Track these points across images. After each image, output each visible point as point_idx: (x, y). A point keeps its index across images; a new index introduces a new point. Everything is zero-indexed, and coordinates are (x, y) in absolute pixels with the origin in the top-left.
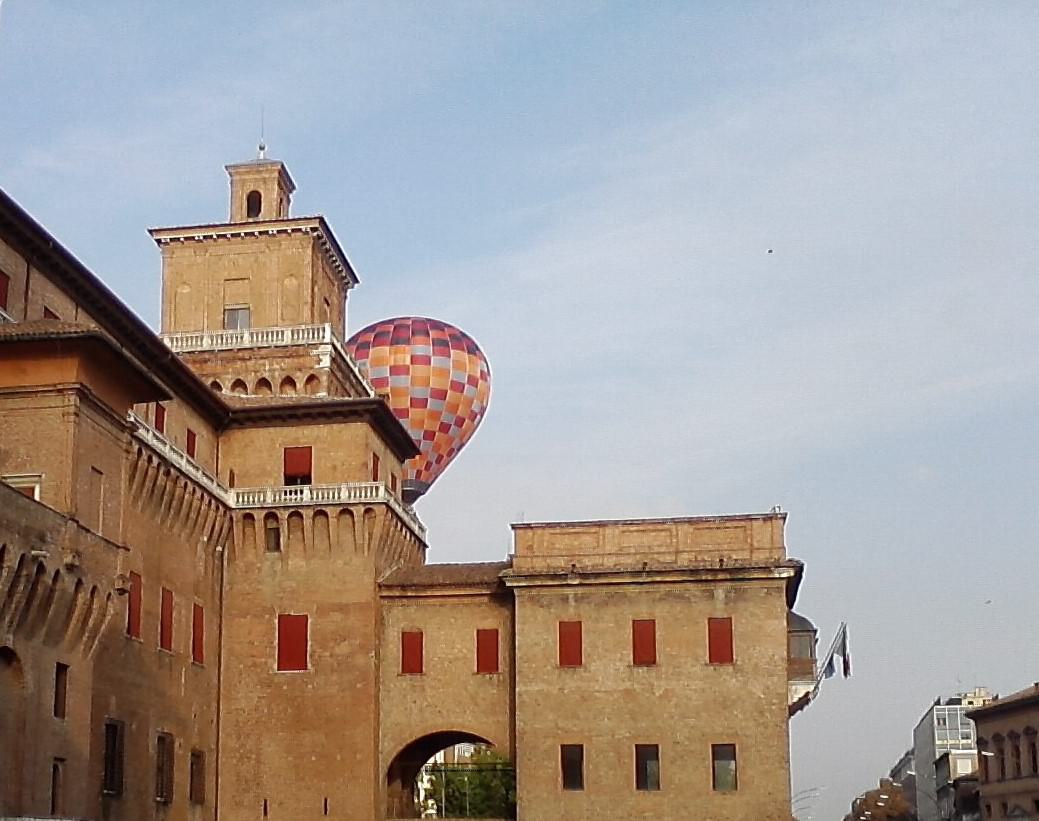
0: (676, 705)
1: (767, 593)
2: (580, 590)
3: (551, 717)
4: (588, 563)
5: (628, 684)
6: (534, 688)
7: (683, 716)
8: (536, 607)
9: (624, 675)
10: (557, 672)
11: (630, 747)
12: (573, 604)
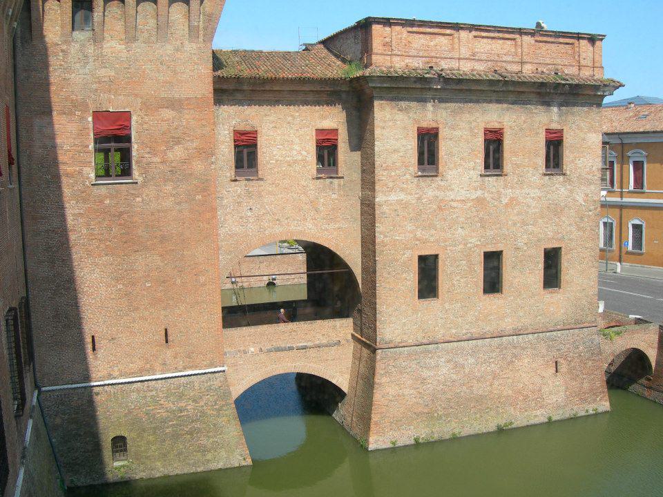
0: (519, 214)
3: (410, 227)
5: (479, 193)
6: (393, 197)
7: (524, 223)
9: (477, 184)
12: (431, 109)
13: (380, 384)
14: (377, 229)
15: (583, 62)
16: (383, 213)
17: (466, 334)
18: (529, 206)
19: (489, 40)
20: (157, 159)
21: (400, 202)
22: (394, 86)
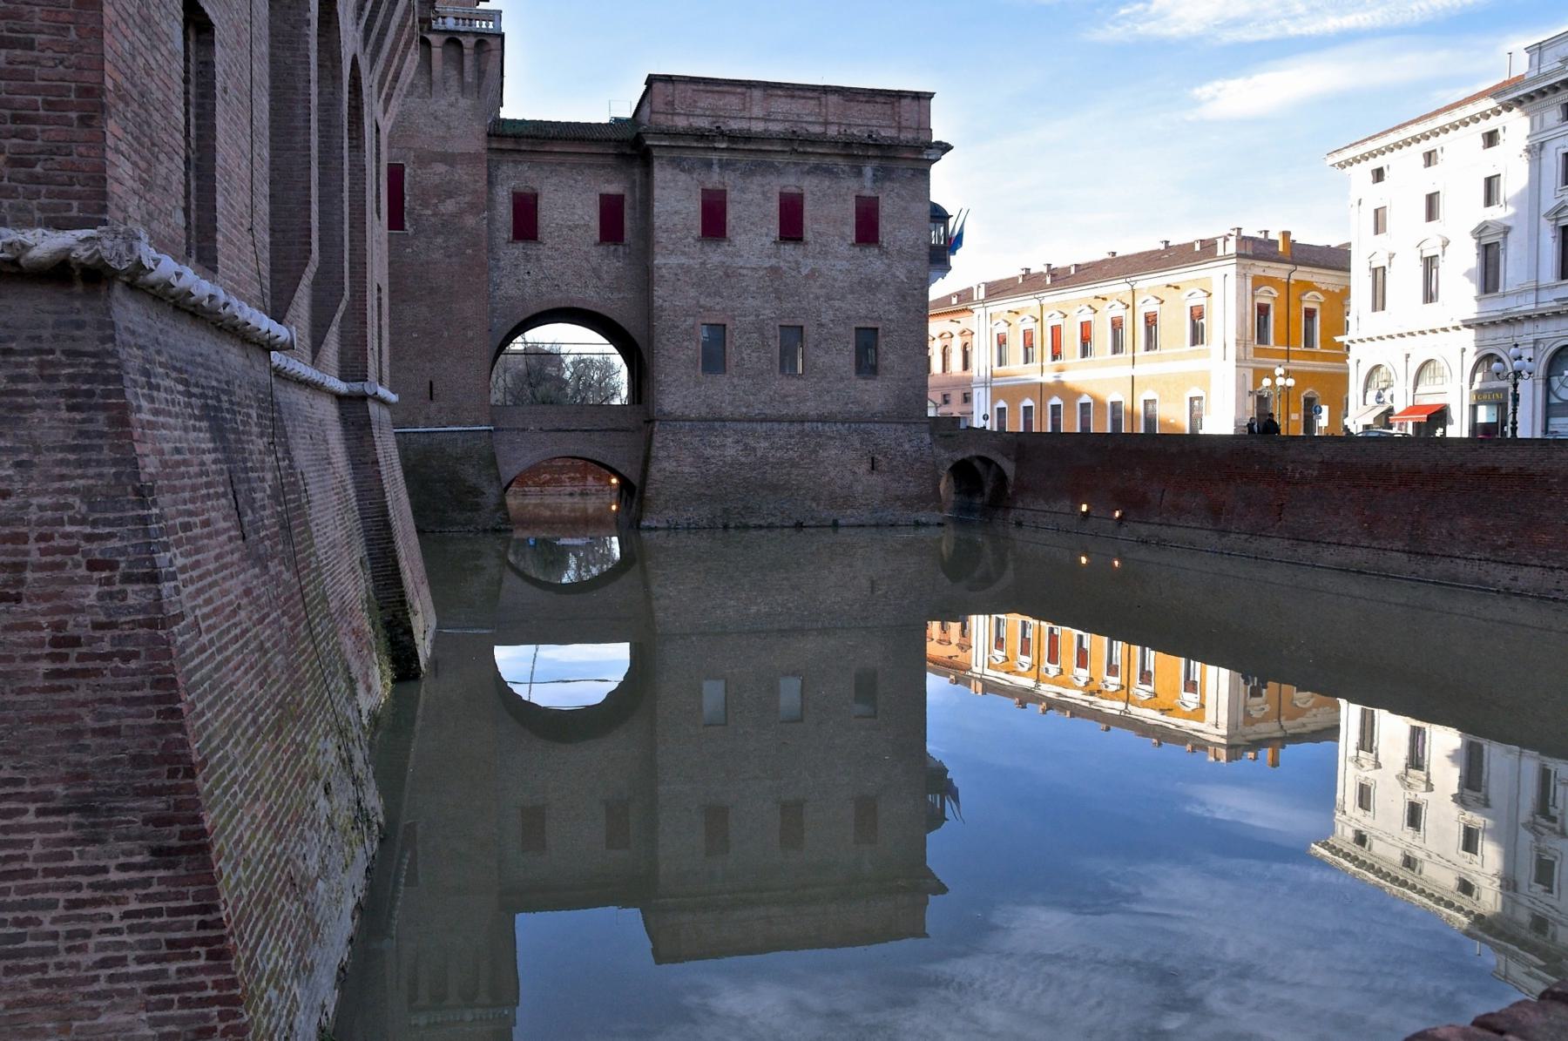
0: (822, 286)
1: (913, 175)
2: (725, 156)
3: (693, 292)
4: (734, 125)
5: (773, 261)
6: (673, 261)
7: (829, 298)
8: (677, 171)
9: (771, 251)
10: (699, 245)
11: (774, 328)
12: (718, 170)
13: (656, 458)
14: (655, 293)
15: (904, 123)
16: (663, 277)
17: (759, 414)
18: (835, 280)
19: (789, 100)
20: (430, 212)
21: (681, 266)
22: (673, 144)
